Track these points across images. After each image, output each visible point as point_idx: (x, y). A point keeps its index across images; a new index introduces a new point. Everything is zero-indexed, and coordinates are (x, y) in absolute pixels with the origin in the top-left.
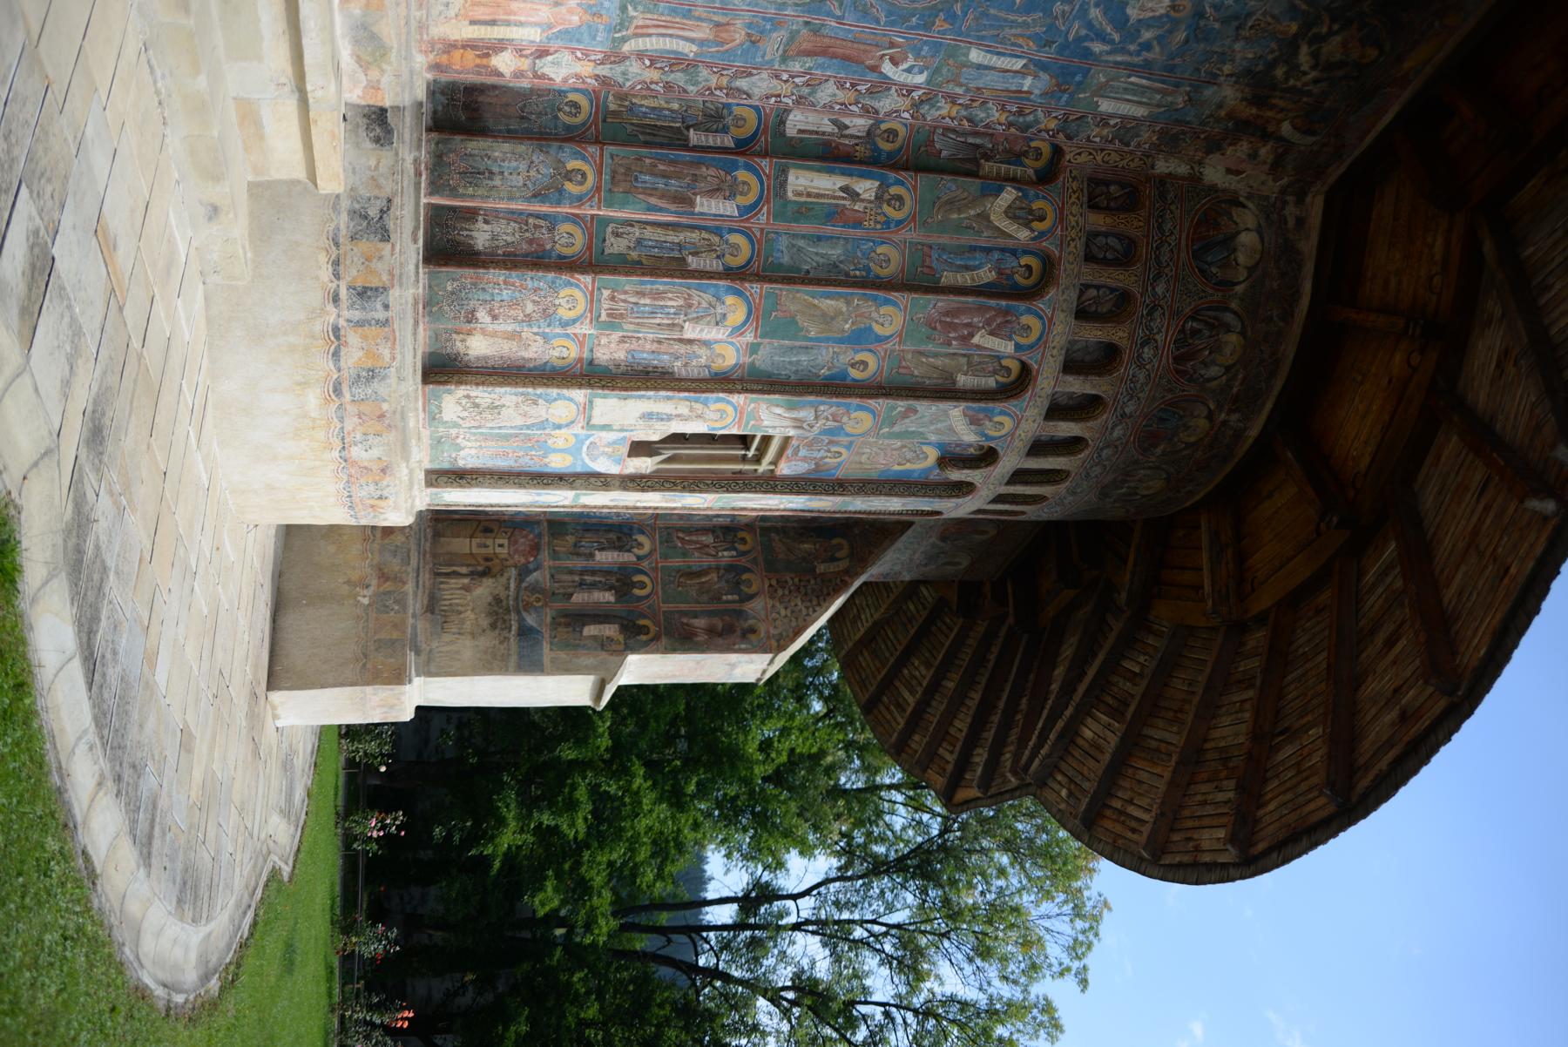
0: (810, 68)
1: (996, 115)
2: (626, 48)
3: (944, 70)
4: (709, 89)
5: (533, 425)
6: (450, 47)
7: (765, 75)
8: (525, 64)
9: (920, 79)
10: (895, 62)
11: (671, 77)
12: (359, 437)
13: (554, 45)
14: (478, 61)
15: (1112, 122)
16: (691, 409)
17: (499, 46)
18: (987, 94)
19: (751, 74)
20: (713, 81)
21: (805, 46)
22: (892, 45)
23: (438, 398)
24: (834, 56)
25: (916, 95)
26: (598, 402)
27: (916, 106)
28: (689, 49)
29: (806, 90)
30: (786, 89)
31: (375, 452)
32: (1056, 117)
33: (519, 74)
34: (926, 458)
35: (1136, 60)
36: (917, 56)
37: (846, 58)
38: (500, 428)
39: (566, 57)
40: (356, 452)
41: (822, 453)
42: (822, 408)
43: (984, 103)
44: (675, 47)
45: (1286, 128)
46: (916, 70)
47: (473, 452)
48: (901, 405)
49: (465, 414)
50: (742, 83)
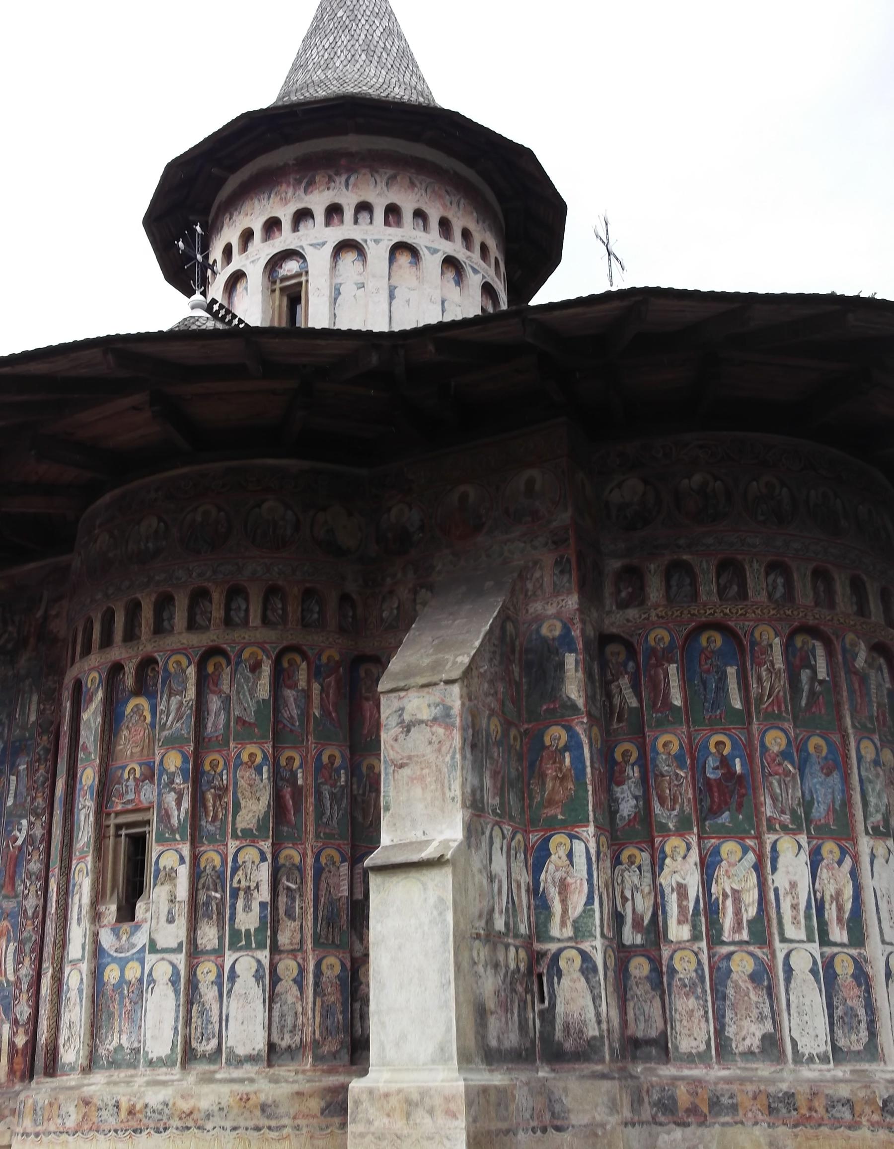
0: (22, 881)
1: (42, 771)
2: (11, 978)
3: (19, 813)
4: (34, 929)
5: (80, 998)
6: (11, 1071)
7: (25, 903)
8: (21, 1030)
9: (24, 822)
10: (16, 839)
11: (27, 950)
12: (59, 1121)
13: (12, 1016)
14: (19, 1055)
15: (42, 707)
16: (77, 893)
17: (12, 1045)
18: (30, 784)
19: (26, 910)
20: (30, 928)
21: (10, 888)
22: (8, 846)
23: (64, 1065)
24: (15, 872)
25: (33, 819)
26: (70, 958)
27: (38, 816)
28: (12, 946)
29: (33, 877)
30: (33, 889)
31: (72, 1110)
32: (41, 739)
33: (26, 1032)
34: (137, 706)
35: (7, 722)
36: (12, 831)
37: (15, 866)
38: (81, 1021)
39: (18, 1009)
40: (71, 1123)
41: (131, 783)
42: (80, 807)
43: (35, 782)
44: (12, 954)
45: (39, 614)
46: (20, 827)
47: (124, 1037)
48: (81, 755)
49: (72, 1046)
50: (30, 913)
